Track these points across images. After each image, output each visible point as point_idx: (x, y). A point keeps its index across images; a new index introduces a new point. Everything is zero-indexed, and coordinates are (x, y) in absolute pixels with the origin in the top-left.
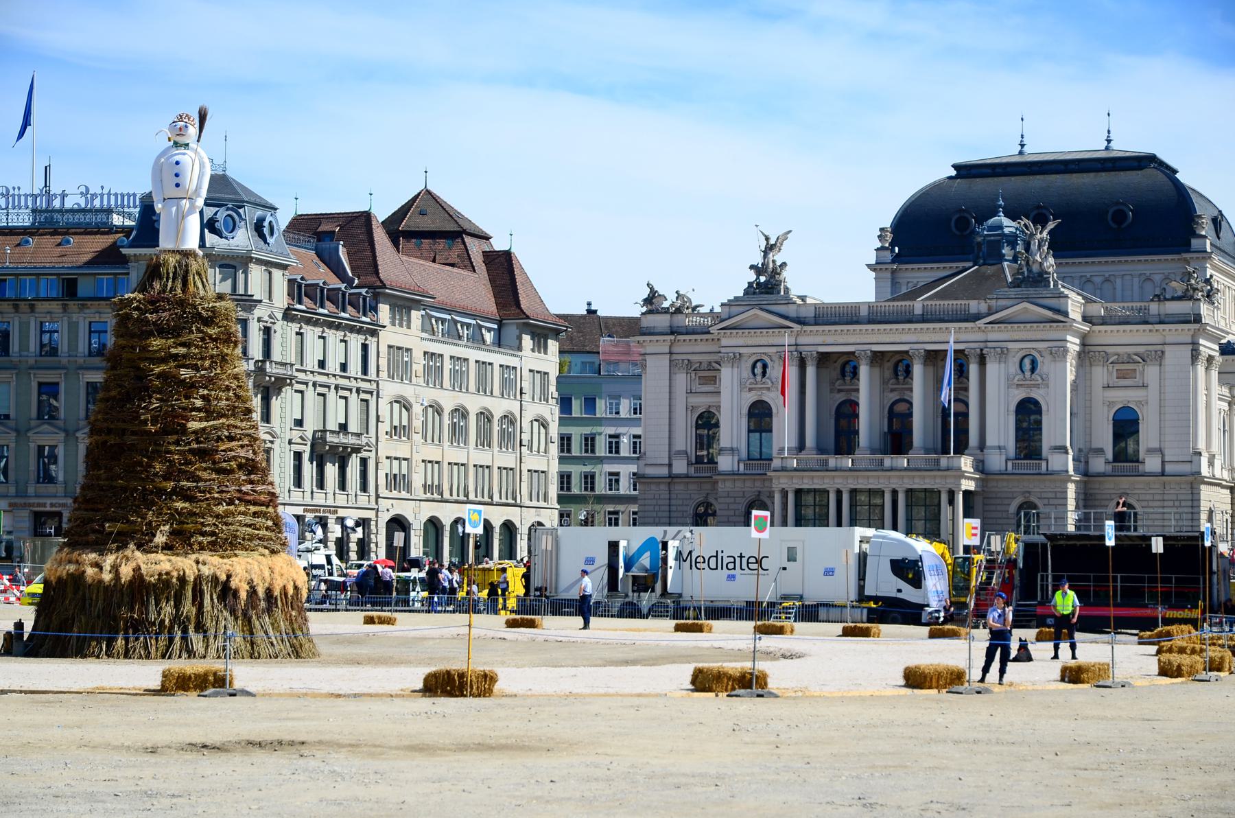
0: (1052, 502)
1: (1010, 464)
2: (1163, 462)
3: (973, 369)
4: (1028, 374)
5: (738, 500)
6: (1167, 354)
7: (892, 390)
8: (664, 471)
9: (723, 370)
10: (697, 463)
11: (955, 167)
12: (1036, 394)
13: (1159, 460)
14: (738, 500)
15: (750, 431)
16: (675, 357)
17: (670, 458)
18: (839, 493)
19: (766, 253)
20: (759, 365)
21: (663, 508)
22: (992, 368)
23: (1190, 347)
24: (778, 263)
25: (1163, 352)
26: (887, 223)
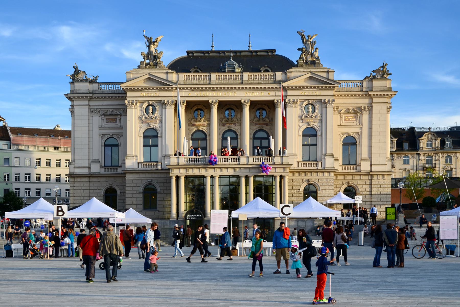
1: (300, 164)
2: (371, 165)
3: (279, 111)
4: (310, 114)
5: (138, 185)
7: (224, 125)
8: (86, 171)
9: (128, 111)
10: (105, 166)
11: (188, 53)
13: (369, 164)
14: (138, 185)
15: (144, 146)
17: (90, 164)
19: (149, 47)
20: (151, 107)
21: (85, 191)
22: (289, 109)
24: (158, 52)
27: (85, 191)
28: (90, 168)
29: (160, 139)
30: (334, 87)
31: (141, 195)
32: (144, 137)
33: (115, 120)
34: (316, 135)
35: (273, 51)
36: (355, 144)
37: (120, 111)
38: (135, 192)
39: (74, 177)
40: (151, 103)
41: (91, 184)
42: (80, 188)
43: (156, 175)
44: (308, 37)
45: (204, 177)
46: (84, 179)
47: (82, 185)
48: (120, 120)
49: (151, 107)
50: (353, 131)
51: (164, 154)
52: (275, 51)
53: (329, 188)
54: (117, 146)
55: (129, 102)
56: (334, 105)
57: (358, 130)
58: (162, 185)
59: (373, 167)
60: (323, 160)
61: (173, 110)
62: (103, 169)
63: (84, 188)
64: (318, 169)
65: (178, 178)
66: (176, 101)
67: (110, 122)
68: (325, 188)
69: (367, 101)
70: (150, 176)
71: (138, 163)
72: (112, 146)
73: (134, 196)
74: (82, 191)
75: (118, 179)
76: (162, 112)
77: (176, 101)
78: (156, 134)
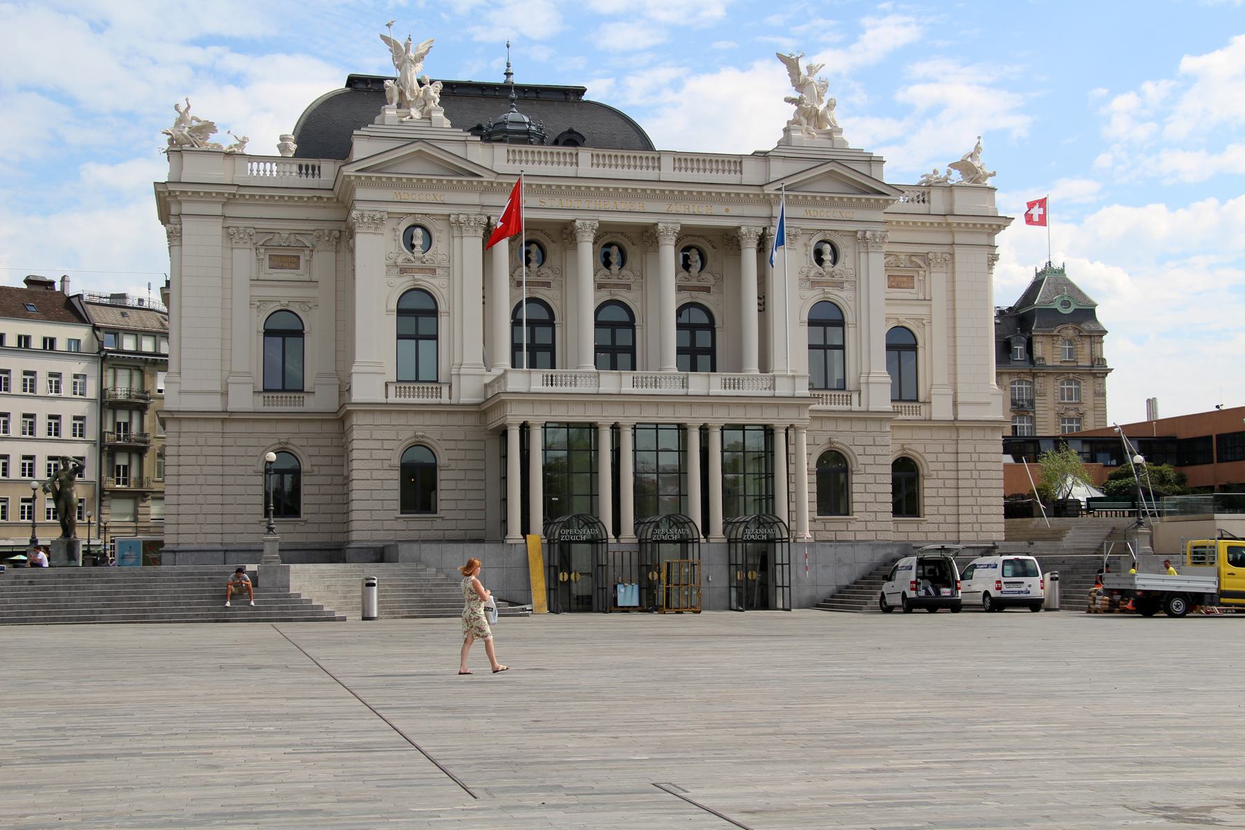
0: (869, 450)
2: (955, 404)
5: (387, 445)
6: (957, 257)
8: (215, 404)
9: (359, 238)
12: (837, 295)
13: (950, 399)
14: (387, 445)
15: (399, 337)
16: (229, 223)
17: (226, 384)
18: (616, 428)
20: (418, 232)
23: (987, 250)
25: (952, 255)
26: (289, 129)
27: (211, 460)
28: (225, 394)
29: (443, 321)
30: (887, 201)
31: (396, 475)
32: (401, 312)
33: (293, 263)
34: (841, 323)
35: (582, 91)
36: (914, 347)
37: (310, 237)
38: (378, 465)
39: (180, 420)
40: (419, 221)
41: (228, 442)
42: (196, 450)
43: (436, 420)
44: (810, 68)
45: (593, 427)
46: (210, 427)
47: (201, 441)
48: (309, 261)
49: (416, 235)
50: (906, 314)
51: (457, 361)
52: (582, 91)
53: (879, 460)
54: (300, 333)
55: (362, 216)
56: (886, 248)
57: (920, 311)
58: (452, 445)
59: (960, 408)
60: (863, 388)
61: (479, 242)
62: (261, 397)
63: (206, 451)
64: (851, 411)
65: (525, 429)
66: (489, 218)
67: (282, 268)
68: (870, 460)
69: (944, 238)
70: (419, 420)
71: (386, 385)
72: (284, 334)
73: (376, 474)
74: (201, 460)
75: (305, 428)
76: (450, 246)
77: (489, 218)
78: (432, 307)
